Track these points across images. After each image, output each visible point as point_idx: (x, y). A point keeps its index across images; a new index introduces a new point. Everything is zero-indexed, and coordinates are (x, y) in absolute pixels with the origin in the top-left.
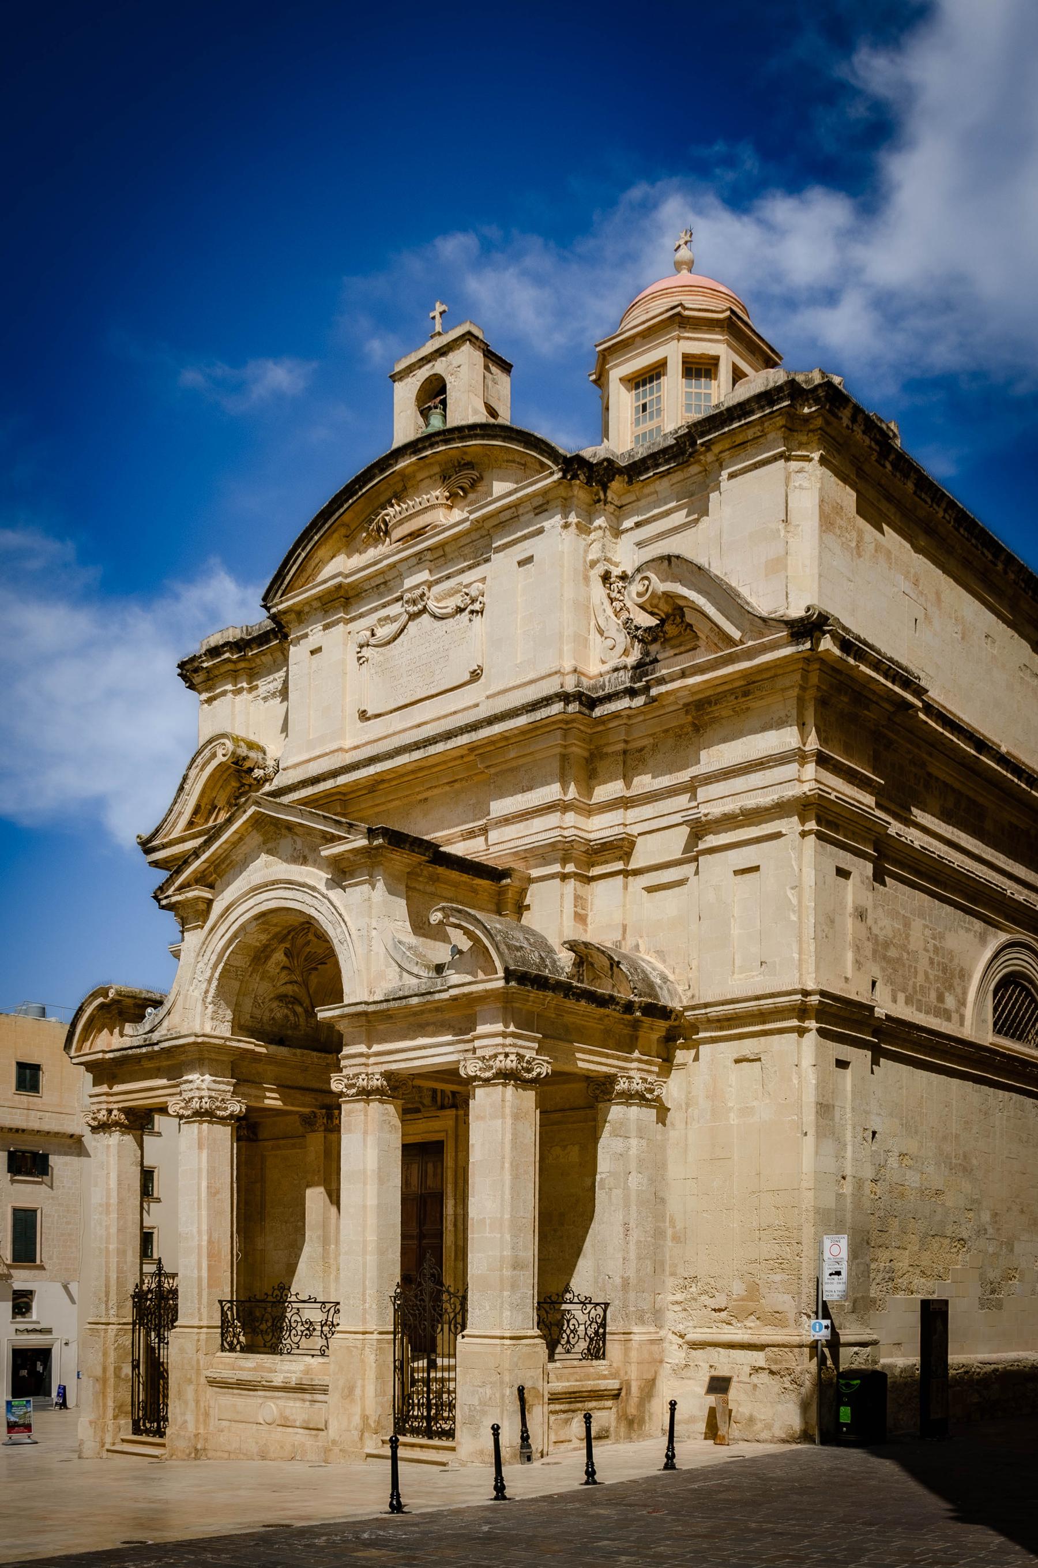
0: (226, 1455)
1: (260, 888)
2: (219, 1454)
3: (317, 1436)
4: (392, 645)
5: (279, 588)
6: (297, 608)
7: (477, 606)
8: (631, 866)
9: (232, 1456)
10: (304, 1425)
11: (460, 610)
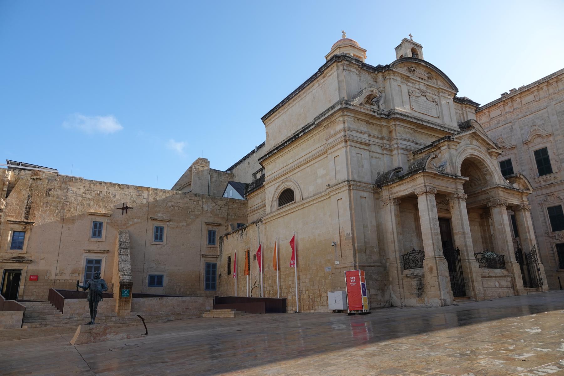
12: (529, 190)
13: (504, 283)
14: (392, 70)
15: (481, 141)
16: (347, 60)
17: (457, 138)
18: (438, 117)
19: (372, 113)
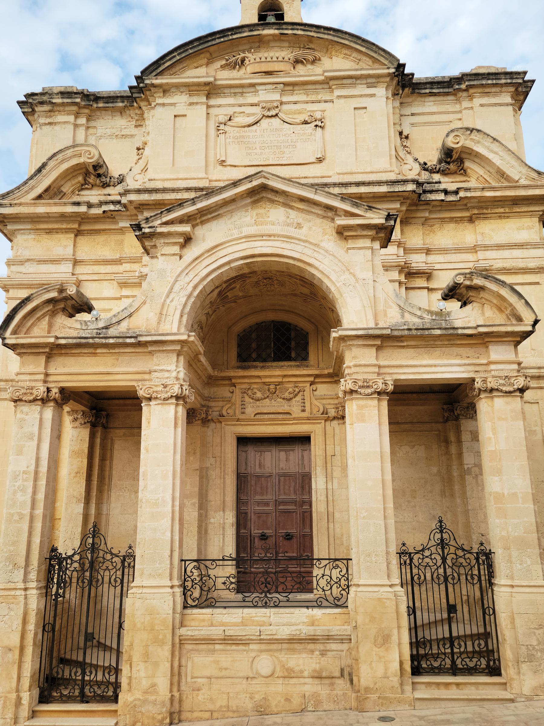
0: (208, 715)
1: (255, 236)
2: (196, 715)
3: (332, 684)
4: (250, 128)
5: (154, 70)
6: (165, 87)
7: (319, 123)
8: (431, 286)
9: (215, 715)
10: (316, 675)
11: (306, 123)
12: (520, 319)
13: (305, 662)
14: (153, 85)
15: (301, 206)
16: (42, 103)
17: (166, 223)
18: (320, 160)
19: (76, 209)
